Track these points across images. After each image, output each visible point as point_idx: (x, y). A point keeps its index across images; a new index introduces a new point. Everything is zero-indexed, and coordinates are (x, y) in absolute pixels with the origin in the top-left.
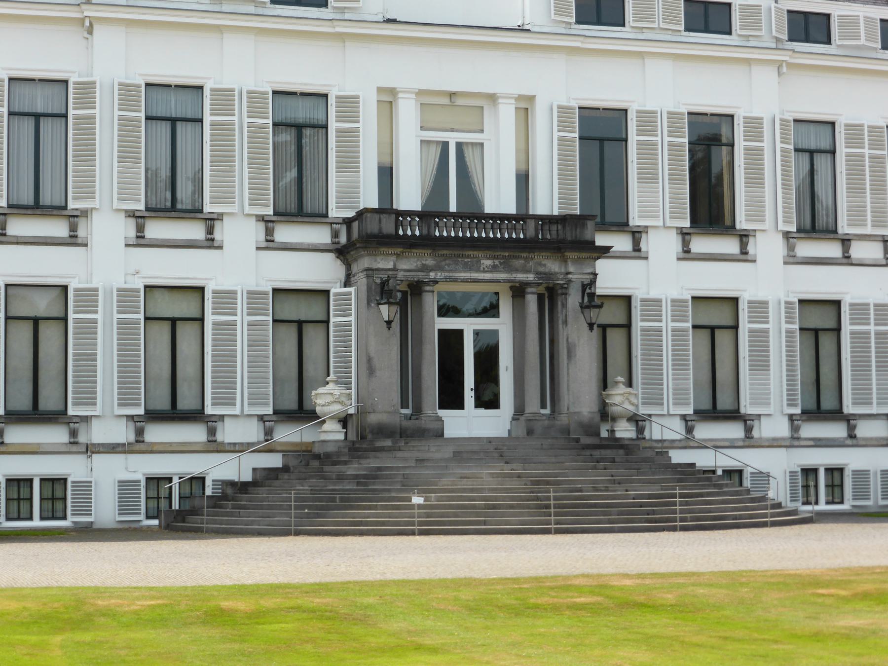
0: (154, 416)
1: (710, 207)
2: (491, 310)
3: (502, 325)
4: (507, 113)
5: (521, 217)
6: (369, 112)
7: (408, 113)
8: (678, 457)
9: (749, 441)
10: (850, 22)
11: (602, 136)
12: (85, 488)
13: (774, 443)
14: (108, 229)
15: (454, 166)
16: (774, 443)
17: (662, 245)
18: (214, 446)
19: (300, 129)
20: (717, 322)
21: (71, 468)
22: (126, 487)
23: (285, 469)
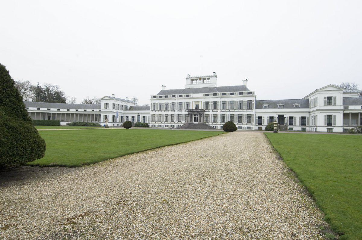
0: (179, 122)
1: (215, 108)
2: (197, 115)
4: (200, 102)
5: (201, 109)
6: (191, 103)
7: (194, 103)
8: (208, 125)
9: (217, 124)
10: (236, 93)
11: (207, 103)
13: (219, 124)
14: (176, 111)
15: (197, 107)
16: (219, 124)
17: (211, 111)
18: (182, 124)
19: (187, 104)
20: (215, 116)
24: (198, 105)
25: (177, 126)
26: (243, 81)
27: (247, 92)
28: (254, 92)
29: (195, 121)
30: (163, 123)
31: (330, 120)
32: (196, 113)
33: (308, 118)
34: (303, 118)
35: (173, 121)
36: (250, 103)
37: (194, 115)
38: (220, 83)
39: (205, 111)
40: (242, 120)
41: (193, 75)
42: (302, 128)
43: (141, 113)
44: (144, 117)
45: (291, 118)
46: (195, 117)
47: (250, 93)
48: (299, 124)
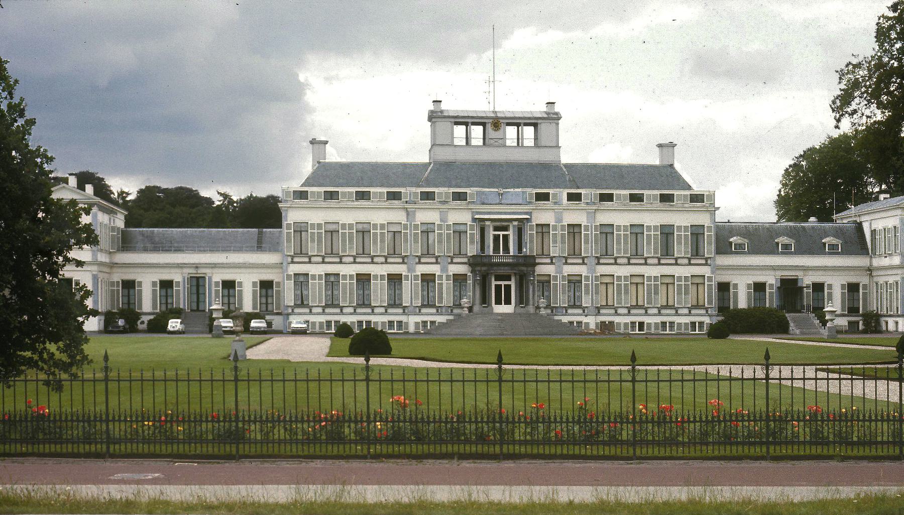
2: (508, 278)
3: (512, 283)
12: (407, 324)
21: (403, 318)
22: (417, 324)
23: (454, 320)
24: (506, 238)
25: (417, 324)
26: (660, 146)
27: (688, 193)
28: (712, 196)
29: (498, 302)
30: (351, 310)
31: (726, 293)
32: (502, 271)
33: (865, 287)
34: (853, 288)
35: (395, 303)
36: (697, 232)
37: (493, 279)
38: (575, 148)
39: (538, 261)
40: (369, 295)
41: (450, 106)
42: (849, 322)
43: (214, 266)
44: (229, 285)
45: (818, 287)
46: (498, 288)
47: (697, 198)
48: (843, 310)
